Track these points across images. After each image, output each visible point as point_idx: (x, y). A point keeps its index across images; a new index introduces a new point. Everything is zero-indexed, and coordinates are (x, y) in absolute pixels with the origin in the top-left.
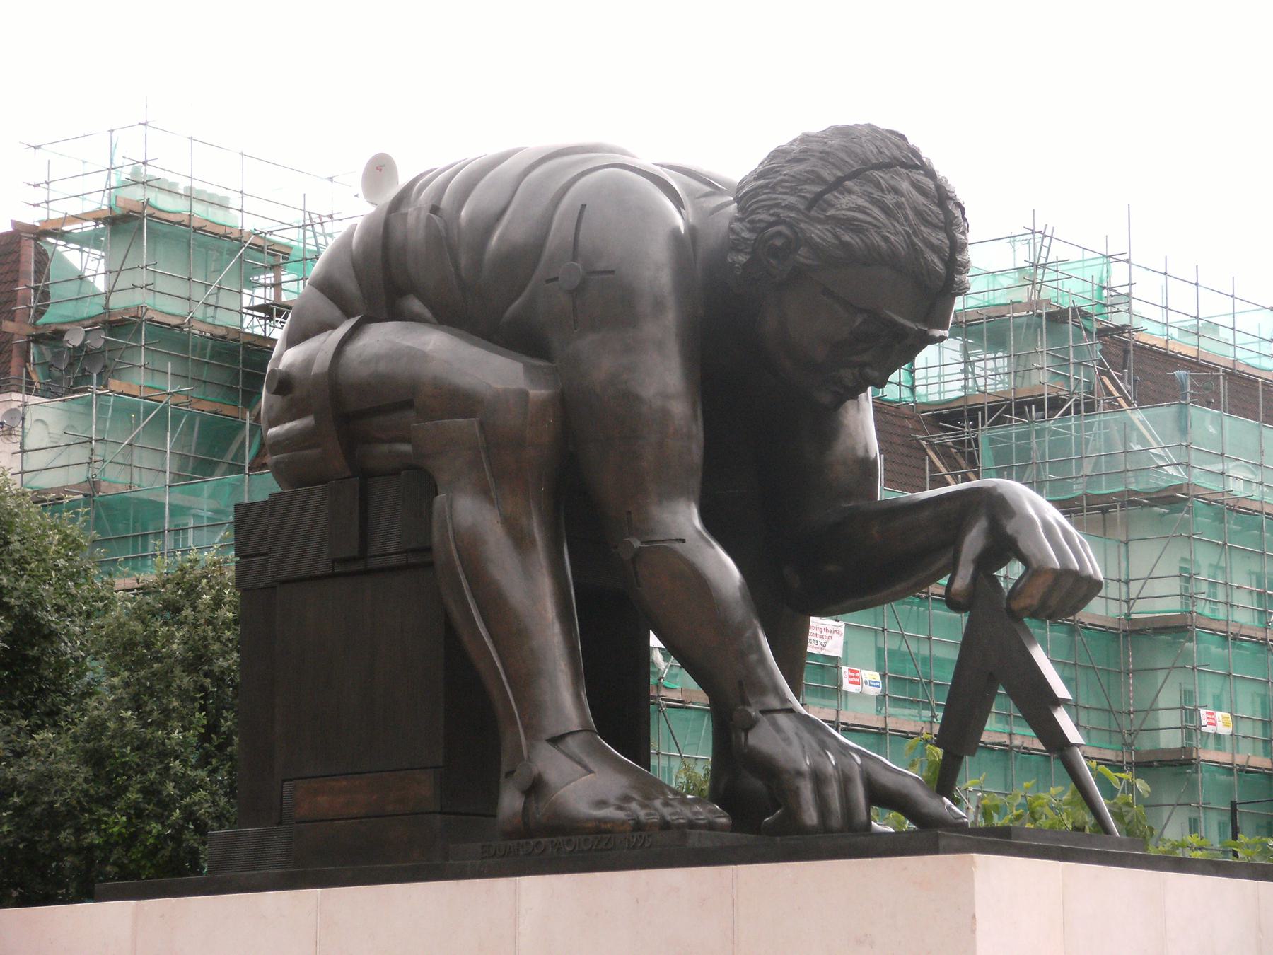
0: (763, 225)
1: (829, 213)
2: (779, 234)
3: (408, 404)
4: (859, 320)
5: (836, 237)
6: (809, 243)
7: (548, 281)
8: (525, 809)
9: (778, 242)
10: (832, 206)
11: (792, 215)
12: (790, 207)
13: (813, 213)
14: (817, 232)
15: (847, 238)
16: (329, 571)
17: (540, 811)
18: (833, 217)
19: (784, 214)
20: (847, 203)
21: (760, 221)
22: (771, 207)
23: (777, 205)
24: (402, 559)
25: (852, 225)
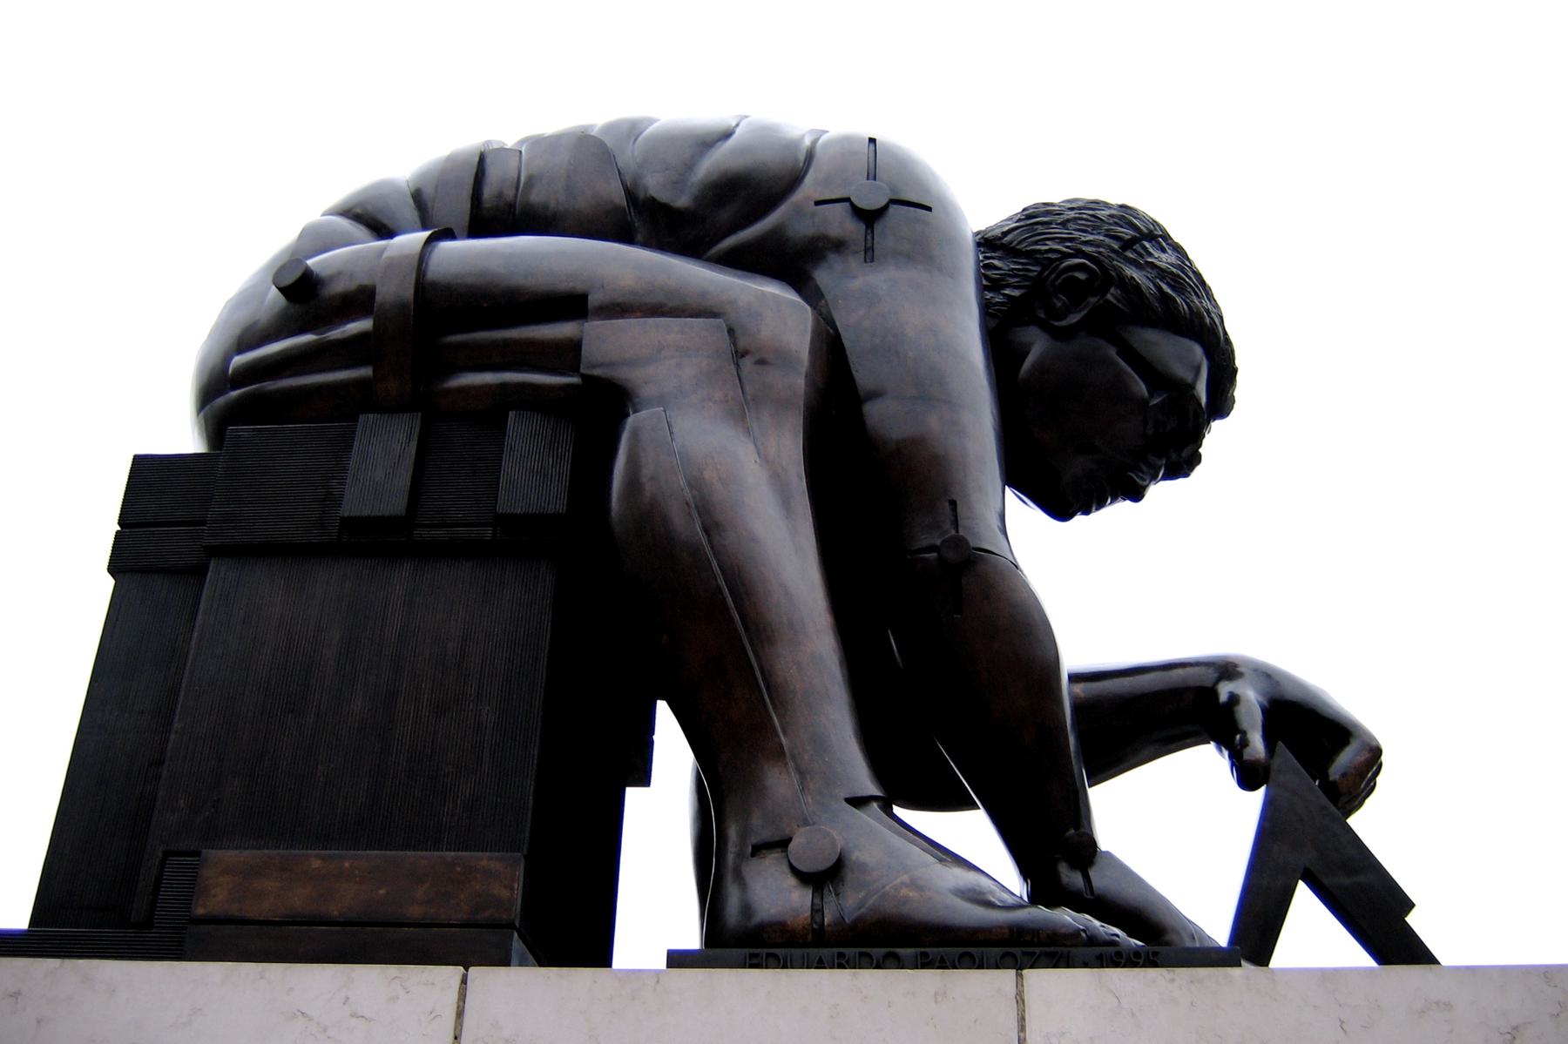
0: (1054, 256)
5: (1159, 288)
7: (818, 203)
8: (817, 910)
9: (1082, 276)
10: (1150, 254)
13: (1129, 254)
18: (1153, 266)
21: (1051, 251)
22: (1063, 240)
23: (1071, 240)
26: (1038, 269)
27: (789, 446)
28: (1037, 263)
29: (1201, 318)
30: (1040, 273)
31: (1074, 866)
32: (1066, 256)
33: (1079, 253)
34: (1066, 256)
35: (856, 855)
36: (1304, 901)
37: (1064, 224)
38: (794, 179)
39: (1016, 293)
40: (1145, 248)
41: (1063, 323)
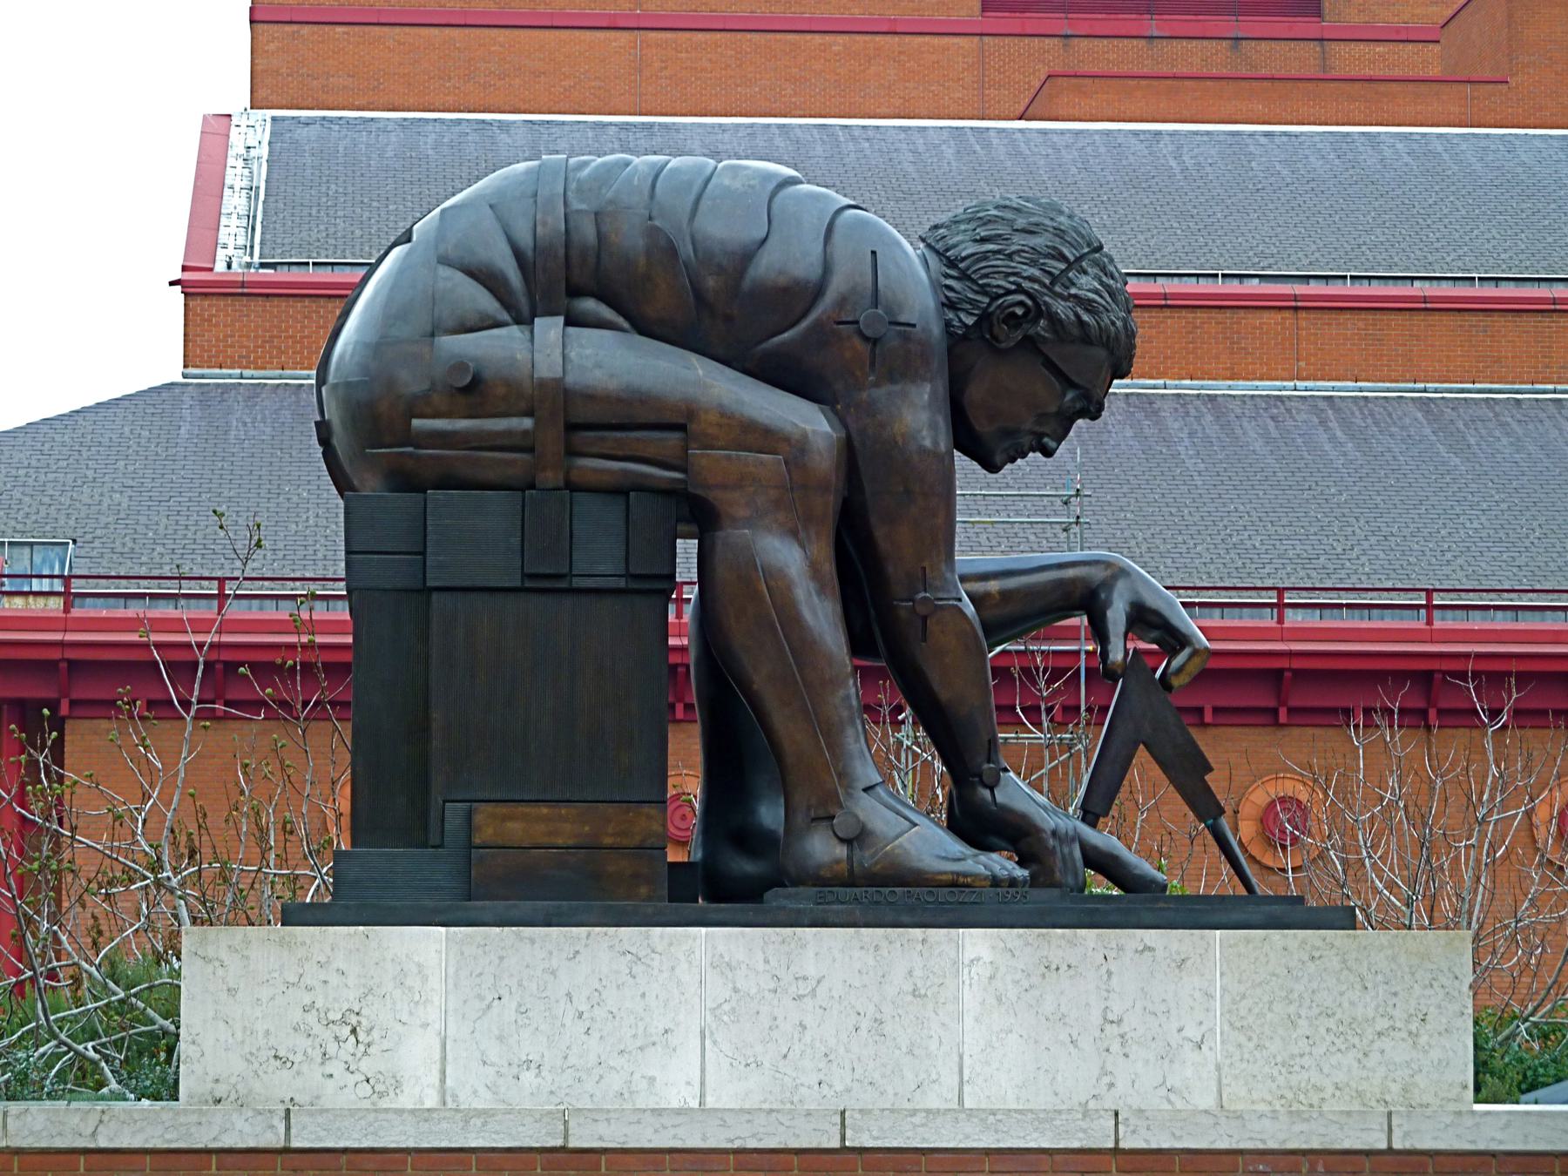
1: (1073, 291)
2: (1021, 303)
3: (681, 428)
4: (1070, 395)
6: (1053, 318)
8: (850, 858)
9: (1019, 311)
11: (1036, 286)
12: (1031, 279)
13: (1058, 289)
14: (1061, 308)
15: (1085, 317)
16: (518, 584)
17: (866, 858)
18: (1075, 296)
19: (1026, 285)
20: (1086, 284)
22: (1008, 275)
24: (622, 583)
25: (1088, 305)
26: (987, 300)
27: (823, 550)
28: (985, 294)
29: (1107, 330)
30: (989, 305)
31: (986, 786)
32: (1009, 292)
33: (1020, 290)
34: (1009, 292)
35: (870, 826)
36: (1142, 754)
37: (1010, 256)
38: (819, 290)
39: (970, 321)
40: (1070, 280)
41: (1003, 345)
